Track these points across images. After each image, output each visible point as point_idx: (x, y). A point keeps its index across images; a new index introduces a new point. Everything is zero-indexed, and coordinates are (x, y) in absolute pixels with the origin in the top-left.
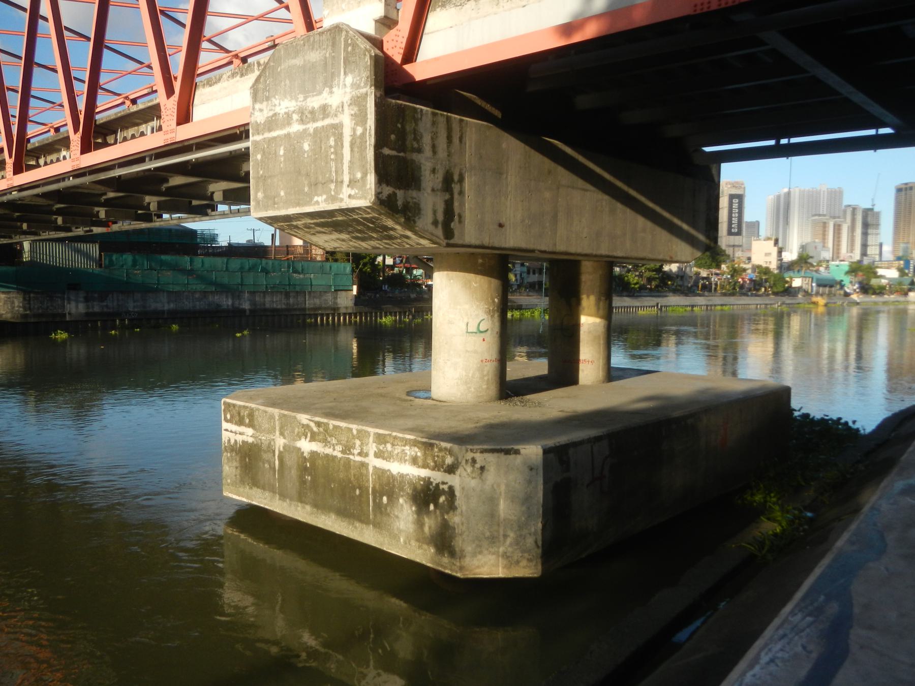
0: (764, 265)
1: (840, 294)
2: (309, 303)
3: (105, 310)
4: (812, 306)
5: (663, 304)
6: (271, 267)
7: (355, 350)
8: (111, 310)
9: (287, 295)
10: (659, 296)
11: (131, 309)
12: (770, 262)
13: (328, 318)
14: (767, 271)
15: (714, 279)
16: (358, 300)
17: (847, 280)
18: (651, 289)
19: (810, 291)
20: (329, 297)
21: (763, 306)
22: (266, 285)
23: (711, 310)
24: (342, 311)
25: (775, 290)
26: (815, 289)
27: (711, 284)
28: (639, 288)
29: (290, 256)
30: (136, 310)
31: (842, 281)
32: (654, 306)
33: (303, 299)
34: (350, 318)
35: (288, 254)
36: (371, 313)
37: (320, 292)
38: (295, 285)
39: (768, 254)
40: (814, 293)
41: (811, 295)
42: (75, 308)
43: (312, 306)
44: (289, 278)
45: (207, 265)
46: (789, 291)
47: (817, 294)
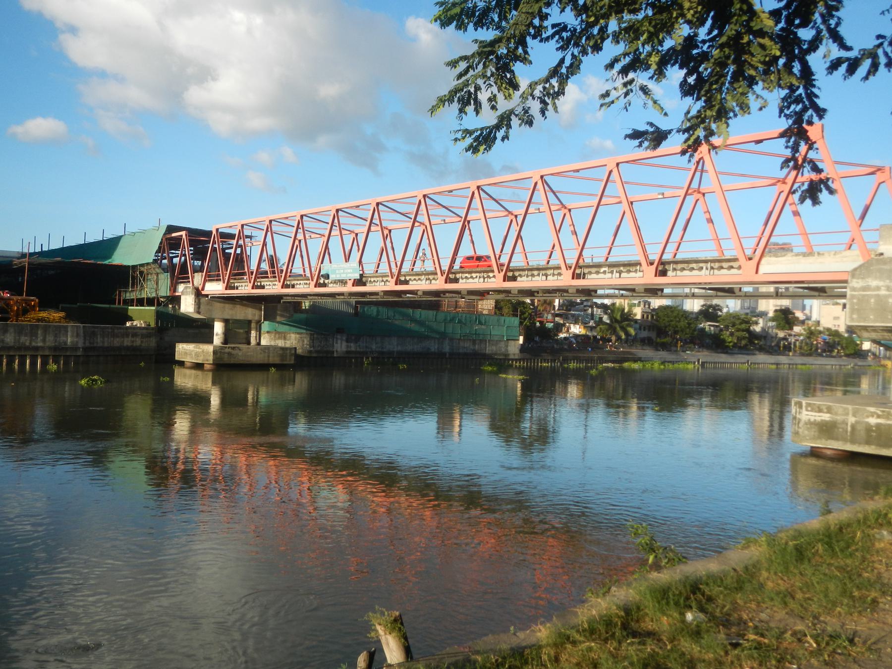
0: (833, 328)
4: (881, 369)
7: (519, 392)
9: (474, 342)
10: (747, 354)
12: (839, 326)
14: (836, 334)
15: (792, 340)
18: (740, 348)
19: (877, 354)
21: (837, 367)
23: (793, 368)
25: (848, 352)
26: (882, 352)
27: (790, 344)
28: (733, 346)
29: (458, 310)
35: (456, 307)
39: (836, 318)
40: (881, 356)
41: (879, 357)
42: (340, 346)
43: (490, 352)
45: (423, 317)
46: (859, 354)
47: (885, 357)
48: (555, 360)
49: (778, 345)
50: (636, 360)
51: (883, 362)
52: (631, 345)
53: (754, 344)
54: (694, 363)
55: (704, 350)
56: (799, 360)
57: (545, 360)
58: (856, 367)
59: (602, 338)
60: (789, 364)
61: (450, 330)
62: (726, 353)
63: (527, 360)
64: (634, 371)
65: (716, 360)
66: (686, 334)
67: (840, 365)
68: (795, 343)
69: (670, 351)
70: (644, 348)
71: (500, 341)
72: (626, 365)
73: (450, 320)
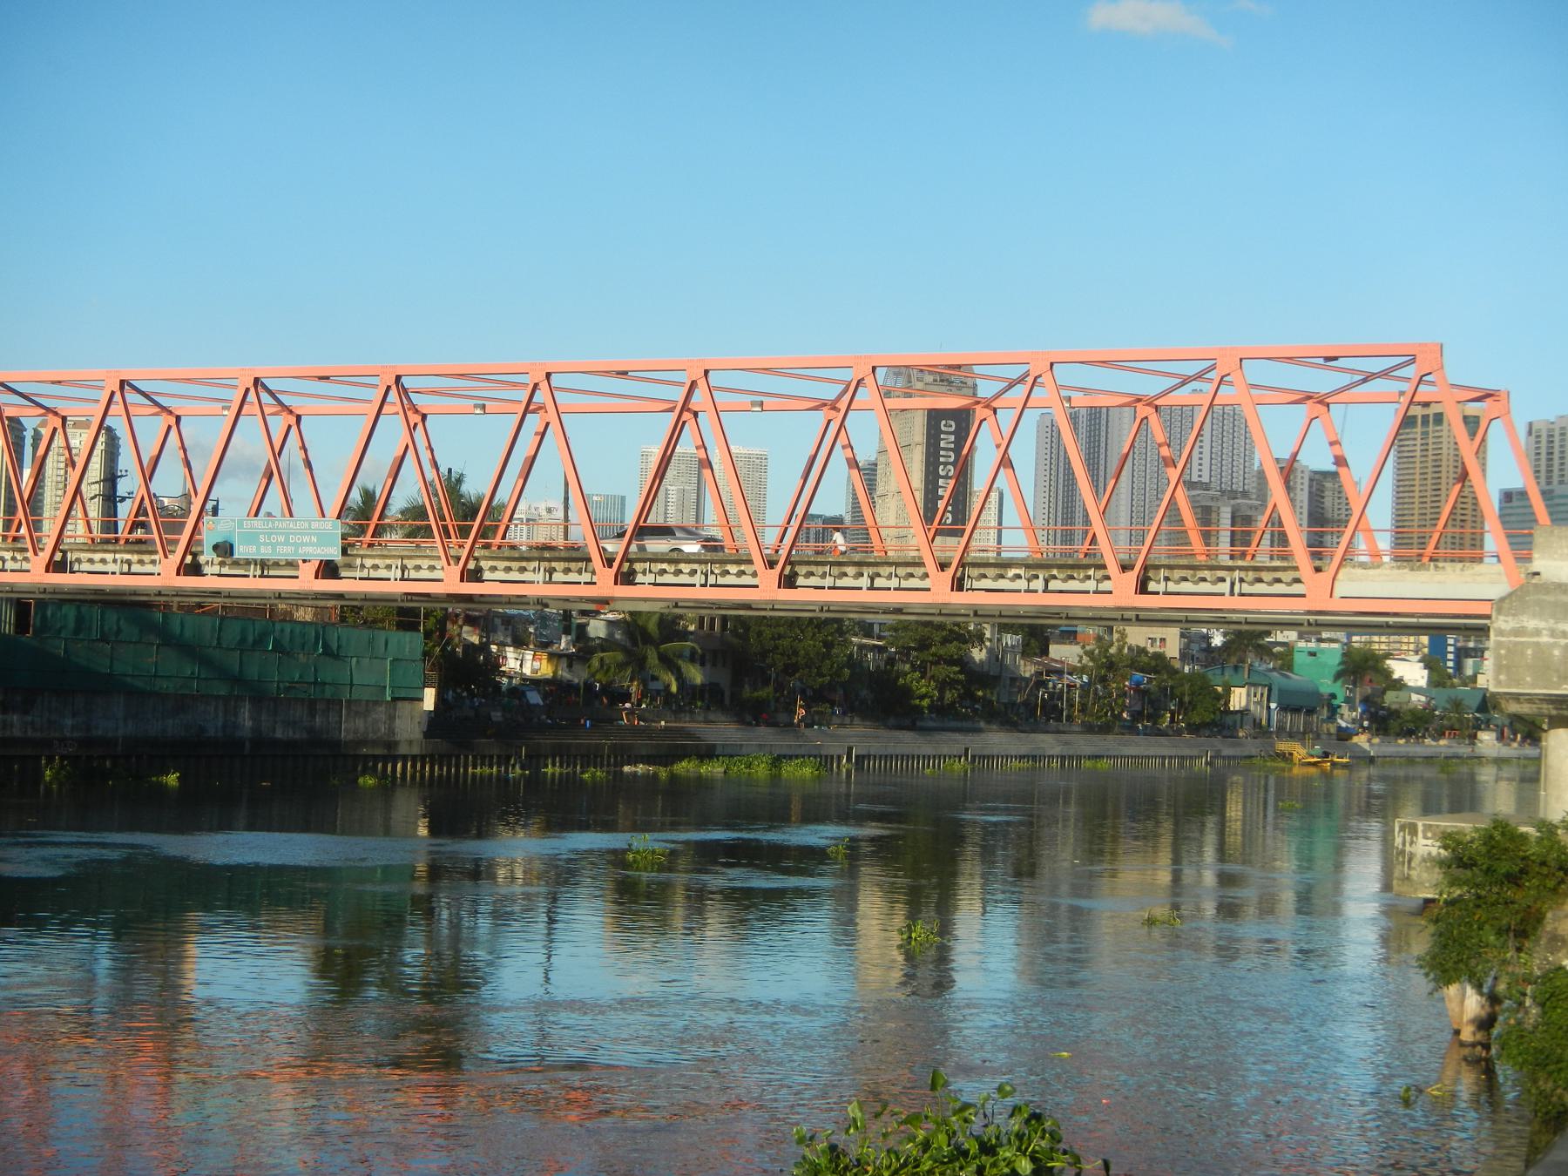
1: (1329, 734)
2: (349, 728)
3: (30, 733)
5: (978, 752)
6: (288, 640)
8: (38, 735)
11: (68, 735)
13: (423, 767)
16: (437, 724)
17: (1340, 691)
20: (380, 713)
22: (278, 682)
24: (403, 750)
30: (75, 735)
31: (1333, 696)
32: (960, 757)
33: (337, 719)
34: (414, 766)
36: (450, 757)
37: (367, 701)
38: (325, 684)
44: (316, 670)
48: (508, 758)
49: (1030, 707)
50: (707, 753)
51: (1283, 746)
52: (680, 710)
53: (975, 699)
54: (839, 758)
55: (857, 720)
56: (1085, 744)
57: (483, 757)
58: (1219, 762)
59: (606, 688)
60: (1063, 758)
61: (252, 672)
62: (912, 727)
63: (432, 757)
64: (702, 783)
65: (890, 751)
66: (823, 676)
67: (1182, 757)
68: (1071, 705)
69: (775, 725)
70: (712, 717)
71: (376, 703)
72: (684, 767)
73: (255, 643)
